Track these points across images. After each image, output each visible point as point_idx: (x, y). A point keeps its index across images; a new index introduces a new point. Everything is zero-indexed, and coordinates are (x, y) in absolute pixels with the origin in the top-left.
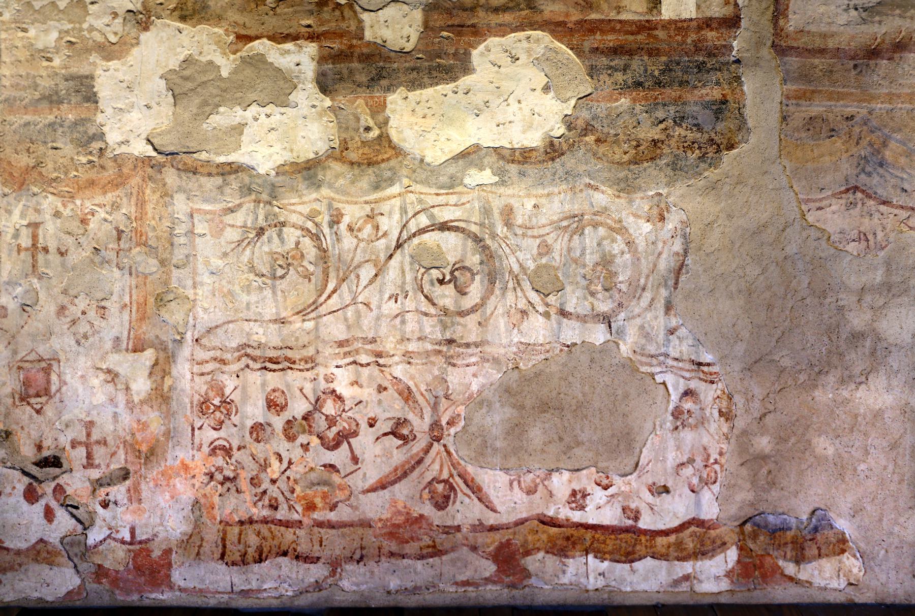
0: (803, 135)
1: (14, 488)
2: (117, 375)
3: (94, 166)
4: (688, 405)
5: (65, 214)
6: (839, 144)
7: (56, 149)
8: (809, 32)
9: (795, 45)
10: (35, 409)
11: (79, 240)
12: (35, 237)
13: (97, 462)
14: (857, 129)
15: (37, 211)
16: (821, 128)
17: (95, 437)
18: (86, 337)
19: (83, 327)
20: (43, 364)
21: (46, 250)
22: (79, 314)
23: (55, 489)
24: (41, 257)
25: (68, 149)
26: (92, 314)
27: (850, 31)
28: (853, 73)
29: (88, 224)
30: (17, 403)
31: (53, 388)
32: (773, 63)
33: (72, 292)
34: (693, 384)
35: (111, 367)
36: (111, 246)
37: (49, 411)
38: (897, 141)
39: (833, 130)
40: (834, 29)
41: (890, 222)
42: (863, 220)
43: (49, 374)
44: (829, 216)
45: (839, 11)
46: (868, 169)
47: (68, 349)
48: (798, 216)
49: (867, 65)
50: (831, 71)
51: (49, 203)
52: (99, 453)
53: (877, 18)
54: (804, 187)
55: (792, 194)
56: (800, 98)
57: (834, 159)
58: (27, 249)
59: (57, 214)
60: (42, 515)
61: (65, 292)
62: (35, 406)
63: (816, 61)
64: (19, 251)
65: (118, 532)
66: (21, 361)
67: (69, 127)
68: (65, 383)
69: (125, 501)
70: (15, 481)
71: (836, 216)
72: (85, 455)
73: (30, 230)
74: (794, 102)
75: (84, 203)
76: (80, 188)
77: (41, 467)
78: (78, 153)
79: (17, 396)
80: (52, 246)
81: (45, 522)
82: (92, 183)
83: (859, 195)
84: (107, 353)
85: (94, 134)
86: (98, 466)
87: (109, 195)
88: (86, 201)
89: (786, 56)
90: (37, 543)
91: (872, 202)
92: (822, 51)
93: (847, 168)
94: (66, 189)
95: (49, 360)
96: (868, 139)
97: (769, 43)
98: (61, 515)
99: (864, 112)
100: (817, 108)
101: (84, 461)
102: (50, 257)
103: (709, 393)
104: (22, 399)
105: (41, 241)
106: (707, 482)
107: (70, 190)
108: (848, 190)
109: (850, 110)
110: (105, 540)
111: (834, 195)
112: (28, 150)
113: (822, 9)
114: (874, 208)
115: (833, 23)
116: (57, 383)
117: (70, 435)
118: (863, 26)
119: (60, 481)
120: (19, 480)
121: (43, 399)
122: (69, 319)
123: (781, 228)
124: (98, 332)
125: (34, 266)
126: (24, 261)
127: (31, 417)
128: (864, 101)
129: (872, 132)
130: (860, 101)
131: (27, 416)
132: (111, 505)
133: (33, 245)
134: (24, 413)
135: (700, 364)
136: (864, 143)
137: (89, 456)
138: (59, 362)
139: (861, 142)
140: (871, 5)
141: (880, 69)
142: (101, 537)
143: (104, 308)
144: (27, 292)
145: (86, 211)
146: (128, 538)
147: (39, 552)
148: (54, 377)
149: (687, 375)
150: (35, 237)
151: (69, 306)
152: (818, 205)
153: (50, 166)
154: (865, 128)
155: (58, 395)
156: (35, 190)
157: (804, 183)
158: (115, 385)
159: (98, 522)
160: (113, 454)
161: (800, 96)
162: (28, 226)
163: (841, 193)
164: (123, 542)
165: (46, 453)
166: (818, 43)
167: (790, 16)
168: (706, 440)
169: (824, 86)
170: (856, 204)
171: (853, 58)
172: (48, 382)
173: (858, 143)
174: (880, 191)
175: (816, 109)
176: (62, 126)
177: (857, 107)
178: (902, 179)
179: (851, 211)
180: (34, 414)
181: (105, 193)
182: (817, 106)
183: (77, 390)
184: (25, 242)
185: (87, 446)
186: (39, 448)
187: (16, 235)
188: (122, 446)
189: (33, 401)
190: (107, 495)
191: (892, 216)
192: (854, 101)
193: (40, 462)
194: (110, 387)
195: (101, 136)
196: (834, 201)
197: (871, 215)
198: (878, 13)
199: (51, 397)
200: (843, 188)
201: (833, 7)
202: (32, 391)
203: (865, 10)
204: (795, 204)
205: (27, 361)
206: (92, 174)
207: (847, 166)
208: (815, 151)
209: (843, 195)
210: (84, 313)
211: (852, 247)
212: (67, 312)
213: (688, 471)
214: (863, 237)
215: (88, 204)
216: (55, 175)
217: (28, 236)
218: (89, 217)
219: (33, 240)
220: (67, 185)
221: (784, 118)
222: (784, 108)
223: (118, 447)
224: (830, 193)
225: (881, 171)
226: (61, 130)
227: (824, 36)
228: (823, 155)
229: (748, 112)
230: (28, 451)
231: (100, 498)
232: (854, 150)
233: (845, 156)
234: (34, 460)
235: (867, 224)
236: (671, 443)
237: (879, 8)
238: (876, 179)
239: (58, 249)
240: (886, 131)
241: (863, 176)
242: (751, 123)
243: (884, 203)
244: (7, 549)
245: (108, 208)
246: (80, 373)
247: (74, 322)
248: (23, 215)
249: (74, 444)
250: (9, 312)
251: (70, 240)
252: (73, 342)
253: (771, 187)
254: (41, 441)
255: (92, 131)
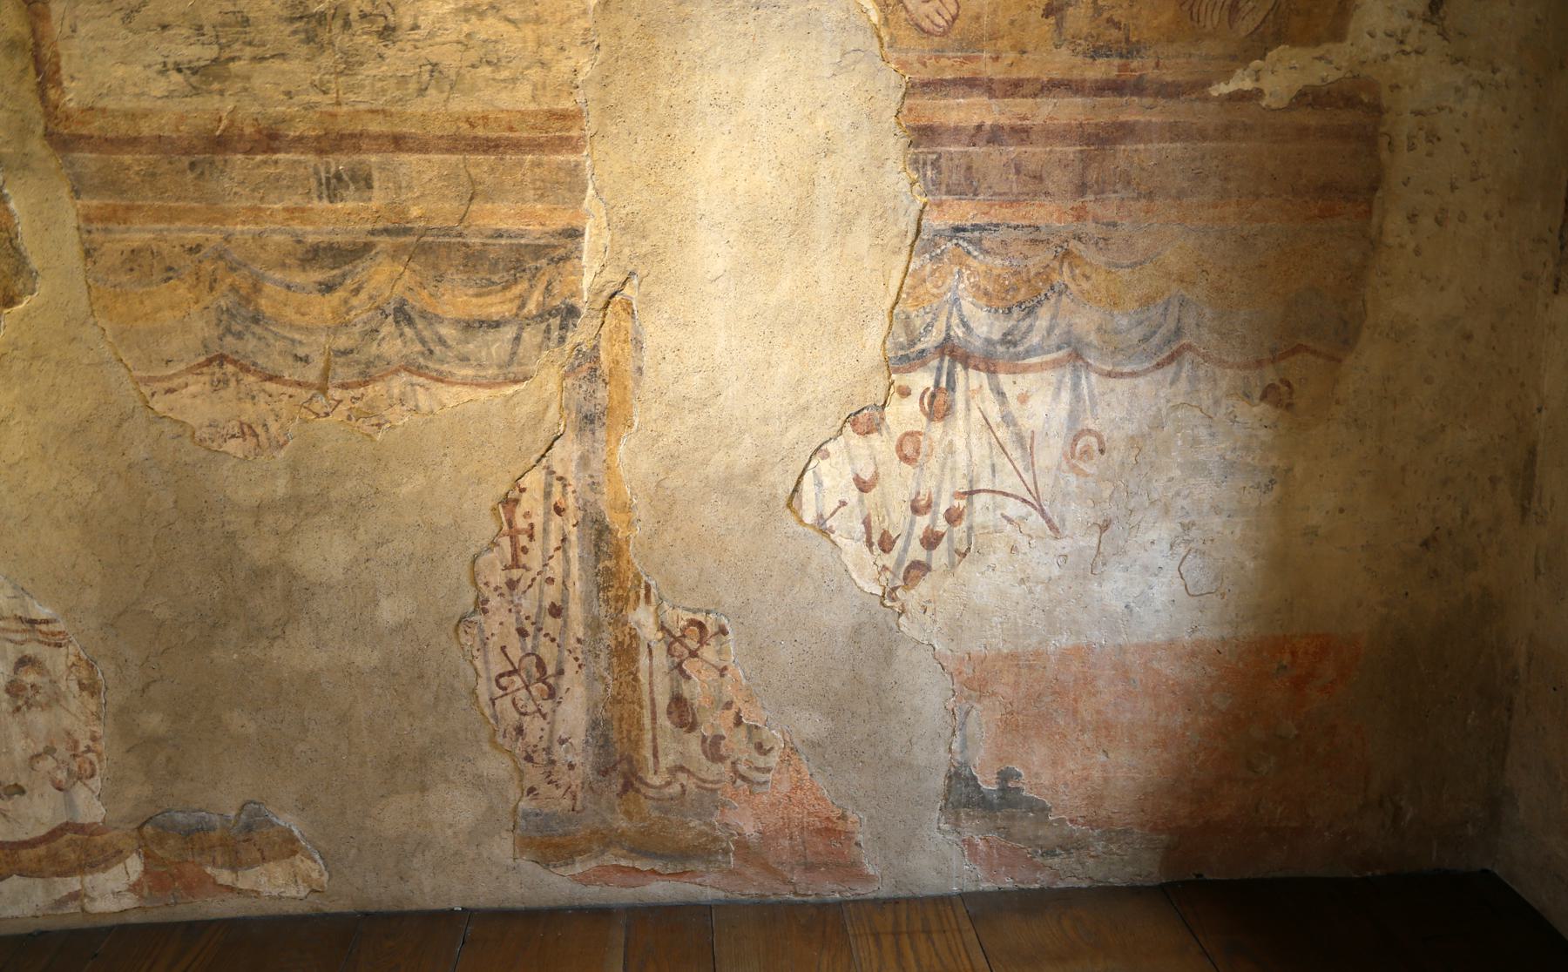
0: (124, 278)
4: (29, 678)
6: (182, 290)
8: (104, 110)
9: (85, 132)
14: (208, 267)
16: (152, 266)
27: (176, 107)
28: (190, 176)
32: (53, 164)
34: (30, 650)
38: (275, 282)
39: (170, 269)
40: (145, 104)
41: (284, 405)
42: (242, 405)
44: (188, 401)
45: (151, 73)
46: (237, 327)
48: (139, 404)
49: (212, 163)
50: (153, 175)
53: (216, 86)
54: (139, 359)
55: (123, 370)
56: (108, 220)
57: (179, 314)
63: (127, 159)
71: (198, 401)
74: (100, 226)
83: (230, 368)
89: (72, 151)
91: (251, 379)
92: (133, 142)
93: (202, 328)
96: (229, 281)
97: (40, 130)
99: (217, 237)
100: (139, 235)
103: (58, 661)
106: (80, 777)
108: (209, 362)
109: (193, 237)
111: (189, 370)
113: (120, 71)
114: (255, 387)
115: (143, 94)
118: (195, 99)
123: (115, 422)
128: (214, 220)
129: (233, 269)
130: (207, 221)
135: (33, 622)
136: (223, 287)
139: (217, 286)
140: (202, 63)
141: (233, 168)
149: (18, 637)
152: (166, 385)
154: (221, 264)
157: (137, 352)
161: (110, 217)
163: (200, 365)
166: (124, 128)
167: (65, 84)
168: (67, 722)
169: (145, 198)
170: (227, 382)
171: (187, 153)
173: (212, 289)
174: (261, 361)
175: (137, 236)
177: (205, 231)
178: (293, 341)
179: (222, 393)
182: (139, 230)
191: (285, 398)
192: (198, 221)
196: (191, 378)
197: (253, 398)
198: (217, 77)
200: (202, 359)
201: (139, 68)
203: (195, 71)
204: (131, 386)
207: (201, 324)
208: (147, 302)
209: (205, 370)
211: (233, 446)
213: (48, 764)
214: (246, 431)
221: (88, 253)
222: (85, 236)
224: (182, 366)
225: (258, 330)
227: (132, 116)
228: (158, 309)
229: (27, 242)
232: (207, 299)
233: (195, 309)
235: (249, 412)
236: (15, 730)
237: (216, 68)
238: (251, 344)
240: (256, 267)
241: (229, 339)
242: (35, 263)
243: (271, 378)
253: (86, 361)
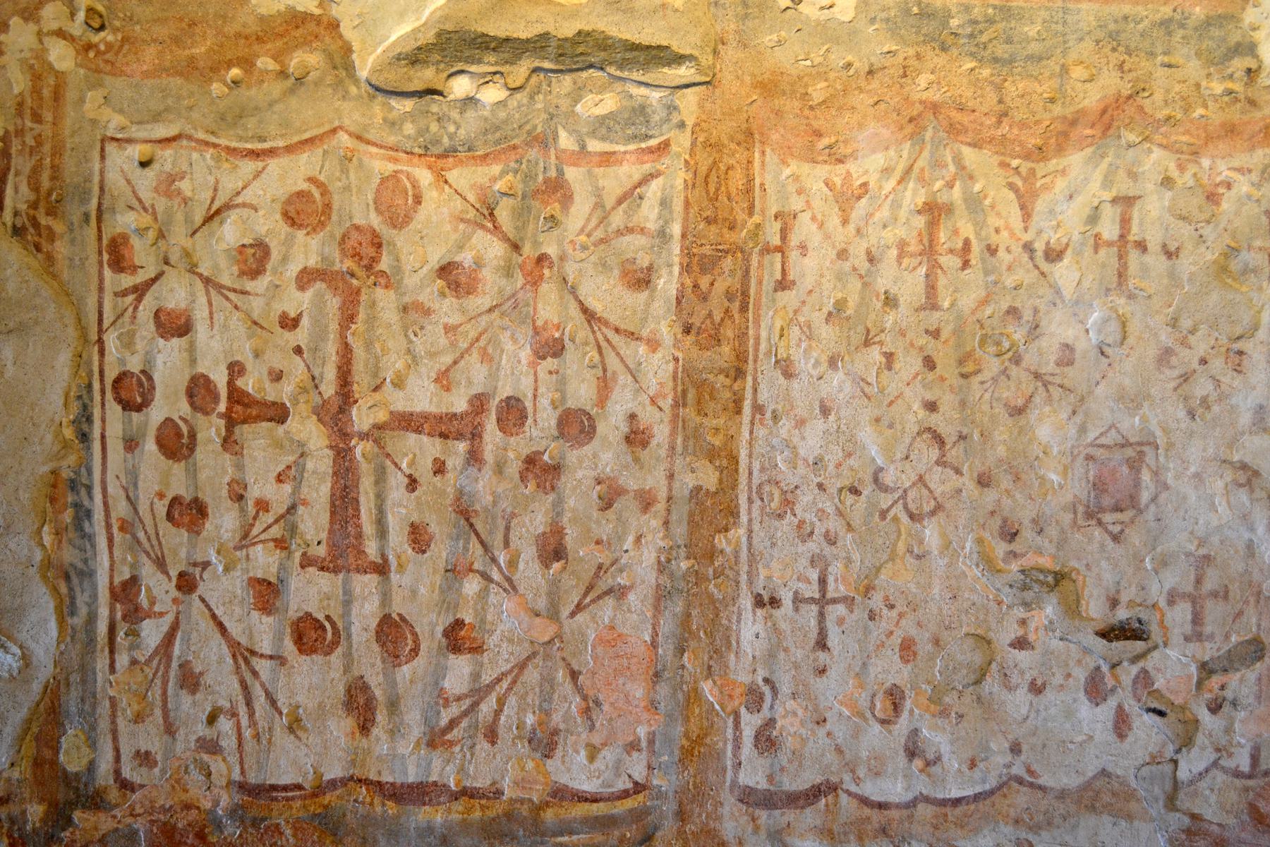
1: (1069, 675)
2: (1256, 473)
3: (1237, 100)
5: (1180, 182)
7: (1170, 66)
10: (1110, 533)
11: (1201, 232)
12: (1125, 222)
13: (1208, 629)
15: (1133, 175)
17: (1208, 586)
18: (1204, 401)
19: (1202, 387)
20: (1130, 452)
21: (1142, 246)
22: (1195, 365)
23: (1137, 677)
24: (1134, 256)
25: (1193, 69)
26: (1217, 364)
29: (1218, 204)
30: (1080, 522)
31: (1145, 496)
33: (1186, 323)
35: (1247, 460)
36: (1258, 243)
37: (1135, 538)
43: (1139, 471)
47: (1173, 426)
51: (1155, 160)
52: (1214, 612)
58: (1110, 244)
59: (1167, 182)
60: (1110, 725)
61: (1174, 323)
62: (1110, 528)
64: (1096, 249)
65: (1230, 755)
66: (1092, 445)
67: (1196, 29)
68: (1166, 487)
69: (1251, 700)
70: (1071, 664)
72: (1189, 617)
73: (1119, 209)
75: (1218, 165)
76: (1209, 139)
77: (1110, 641)
78: (1209, 75)
79: (1081, 509)
80: (1154, 239)
81: (1112, 737)
82: (1231, 130)
84: (1243, 433)
85: (1239, 44)
86: (1211, 637)
87: (1260, 153)
88: (1219, 161)
90: (1094, 777)
94: (1184, 138)
95: (1141, 444)
98: (1144, 724)
101: (1188, 628)
102: (1148, 259)
104: (1089, 515)
105: (1135, 229)
107: (1192, 140)
110: (1207, 771)
112: (1121, 67)
116: (1152, 486)
117: (1171, 579)
119: (1150, 663)
120: (1079, 661)
121: (1126, 516)
122: (1176, 373)
124: (1227, 397)
125: (1120, 275)
126: (1104, 266)
127: (1102, 546)
131: (1096, 545)
132: (1227, 708)
133: (1122, 236)
134: (1090, 540)
137: (1197, 620)
138: (1157, 449)
142: (1201, 766)
143: (1240, 353)
144: (1106, 321)
145: (1218, 179)
146: (1245, 767)
147: (1098, 793)
148: (1146, 476)
150: (1125, 222)
151: (1178, 348)
153: (1158, 97)
155: (1153, 508)
156: (1132, 137)
158: (1252, 491)
159: (1200, 739)
160: (1240, 614)
162: (1114, 201)
164: (1237, 774)
165: (1122, 614)
172: (1137, 484)
176: (1182, 26)
180: (1110, 544)
181: (1252, 148)
183: (1185, 498)
184: (1109, 230)
185: (1194, 600)
186: (1114, 603)
187: (1094, 217)
188: (1252, 600)
189: (1108, 518)
190: (1223, 688)
193: (1113, 629)
194: (1243, 495)
195: (1250, 49)
199: (1141, 512)
202: (1107, 501)
205: (1102, 446)
206: (1235, 114)
210: (1203, 361)
212: (1174, 360)
215: (1222, 166)
216: (1166, 112)
217: (1113, 221)
218: (1221, 190)
219: (1122, 228)
220: (1187, 132)
223: (1246, 602)
226: (1181, 32)
230: (1095, 608)
231: (1208, 696)
234: (1101, 626)
239: (1164, 246)
244: (1041, 788)
245: (1255, 177)
246: (1193, 469)
247: (1186, 378)
248: (1107, 182)
249: (1172, 599)
250: (1078, 355)
251: (1186, 231)
252: (1182, 414)
254: (1118, 592)
255: (1235, 38)
